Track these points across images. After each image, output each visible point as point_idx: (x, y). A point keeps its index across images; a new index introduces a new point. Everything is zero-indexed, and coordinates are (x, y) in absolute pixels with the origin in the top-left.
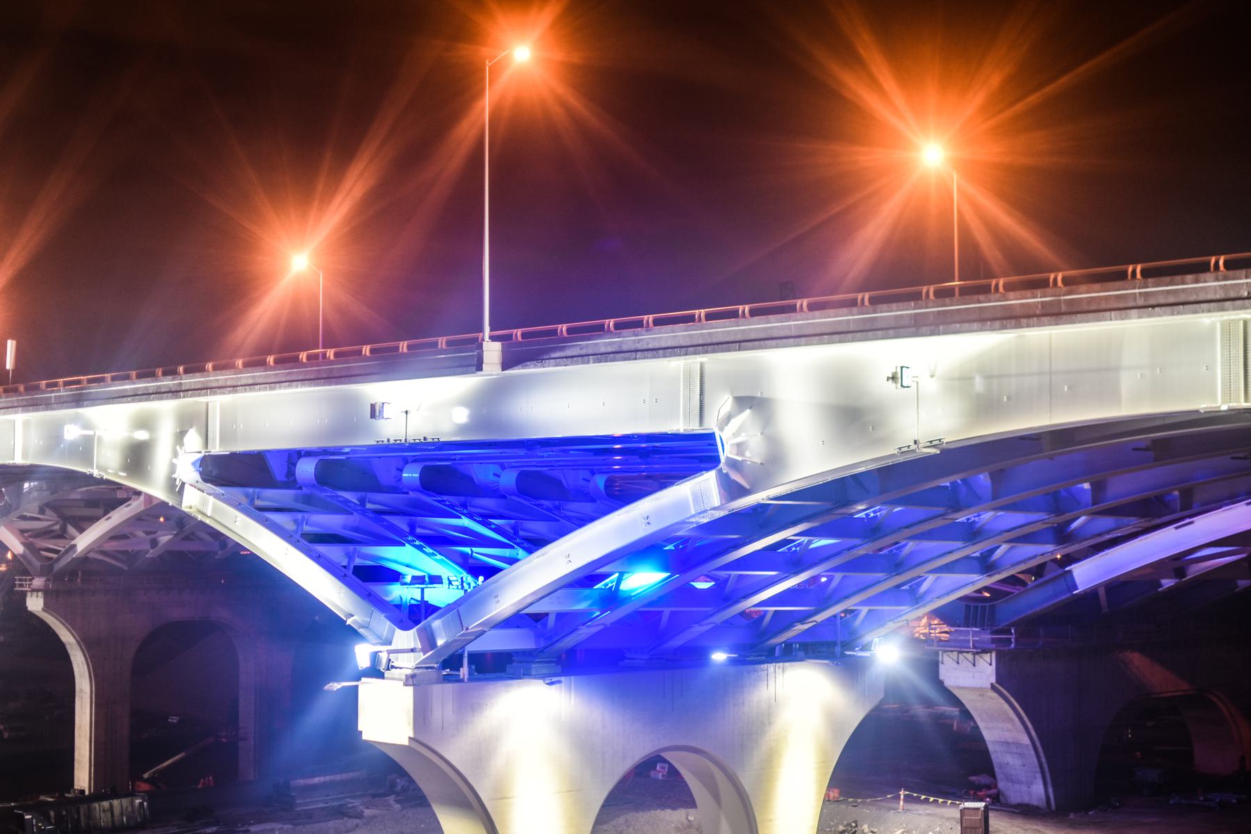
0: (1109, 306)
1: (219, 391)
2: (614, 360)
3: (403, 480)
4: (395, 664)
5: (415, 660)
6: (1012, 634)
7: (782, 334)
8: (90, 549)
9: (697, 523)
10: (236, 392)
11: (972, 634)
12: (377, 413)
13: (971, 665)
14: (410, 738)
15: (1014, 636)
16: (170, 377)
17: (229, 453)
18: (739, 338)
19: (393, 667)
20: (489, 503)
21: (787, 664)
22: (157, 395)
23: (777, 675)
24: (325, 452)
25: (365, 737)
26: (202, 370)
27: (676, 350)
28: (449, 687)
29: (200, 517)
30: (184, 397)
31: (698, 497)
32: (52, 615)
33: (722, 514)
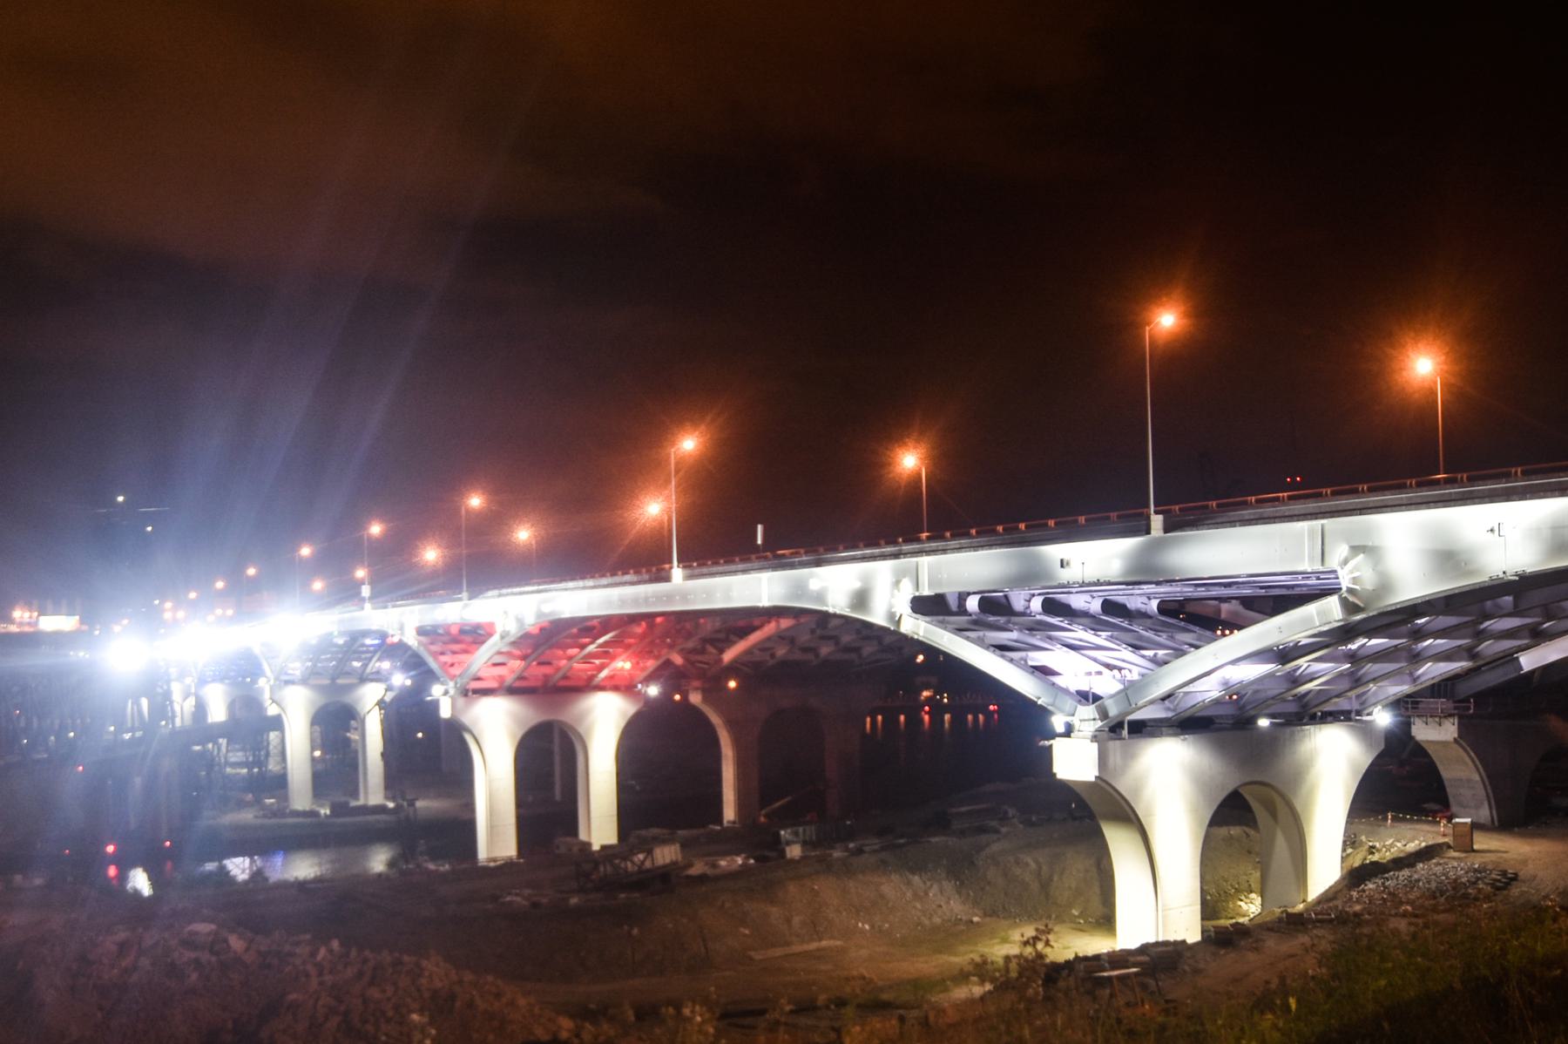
6: (1470, 702)
10: (945, 553)
11: (1441, 703)
12: (1065, 564)
18: (1359, 507)
21: (1323, 726)
26: (918, 540)
28: (1118, 742)
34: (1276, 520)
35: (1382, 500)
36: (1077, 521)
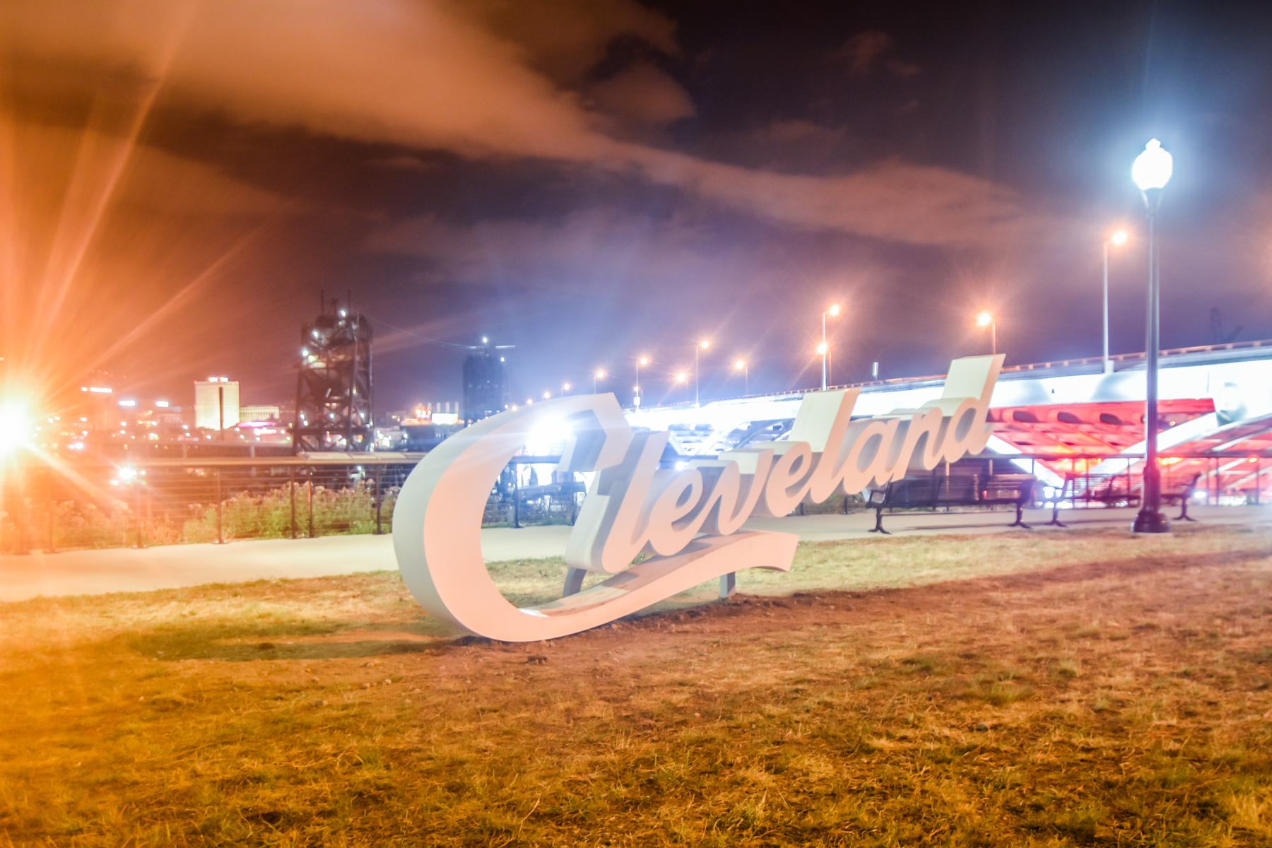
20: (1086, 427)
36: (1061, 365)
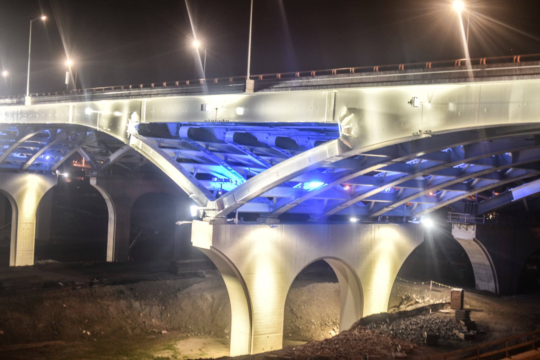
0: (505, 74)
1: (144, 96)
2: (298, 90)
3: (226, 137)
4: (208, 215)
5: (215, 213)
6: (483, 217)
7: (367, 81)
8: (115, 161)
9: (330, 162)
10: (151, 97)
11: (466, 216)
13: (465, 230)
14: (211, 247)
15: (484, 218)
16: (126, 90)
17: (149, 123)
18: (349, 82)
19: (206, 216)
21: (381, 225)
22: (121, 97)
23: (376, 229)
24: (190, 124)
25: (194, 245)
27: (323, 86)
28: (229, 226)
29: (136, 149)
30: (131, 98)
31: (330, 151)
32: (100, 187)
33: (341, 158)
34: (308, 88)
35: (360, 79)
